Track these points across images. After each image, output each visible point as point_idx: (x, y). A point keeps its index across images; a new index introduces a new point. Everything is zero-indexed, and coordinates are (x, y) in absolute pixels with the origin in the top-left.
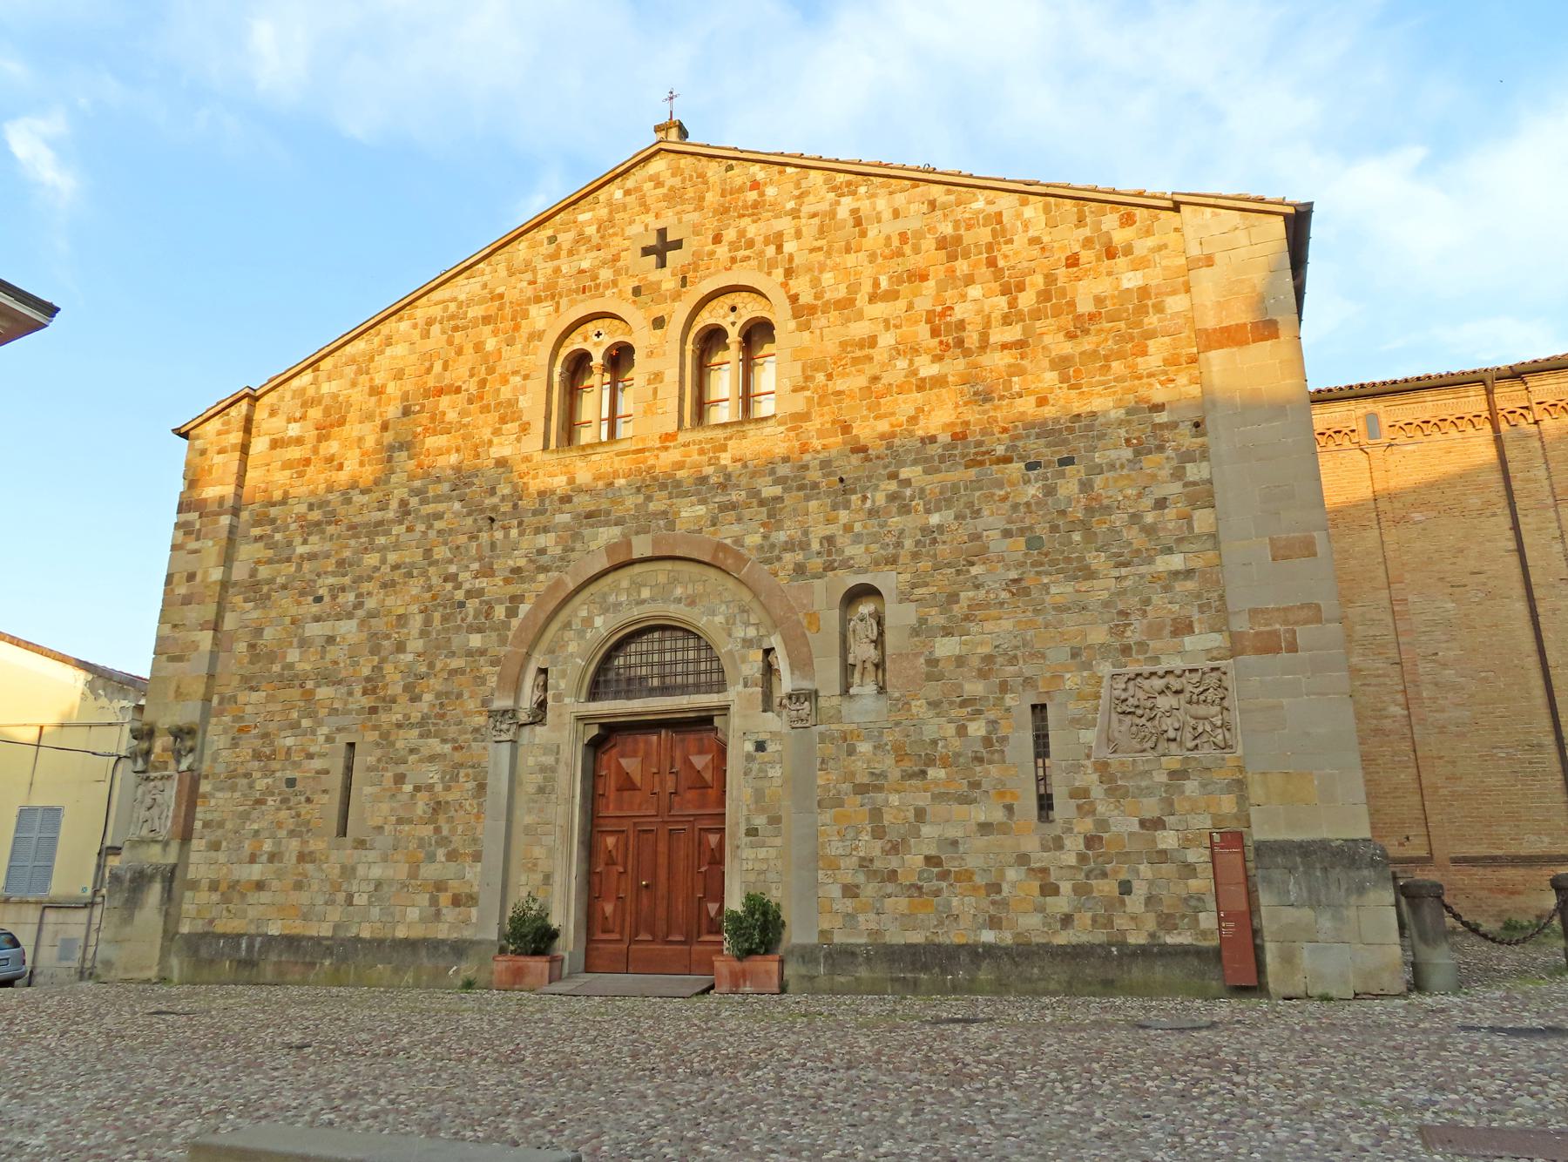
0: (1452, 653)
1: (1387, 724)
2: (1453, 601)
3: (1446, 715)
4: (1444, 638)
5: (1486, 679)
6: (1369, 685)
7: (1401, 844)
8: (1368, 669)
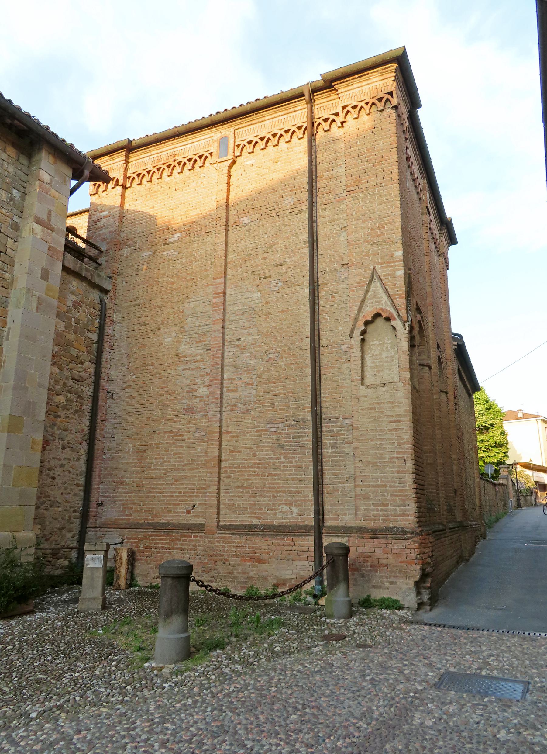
0: (250, 338)
1: (196, 403)
2: (259, 291)
3: (238, 394)
4: (247, 325)
5: (271, 360)
6: (188, 369)
7: (188, 512)
8: (190, 356)
